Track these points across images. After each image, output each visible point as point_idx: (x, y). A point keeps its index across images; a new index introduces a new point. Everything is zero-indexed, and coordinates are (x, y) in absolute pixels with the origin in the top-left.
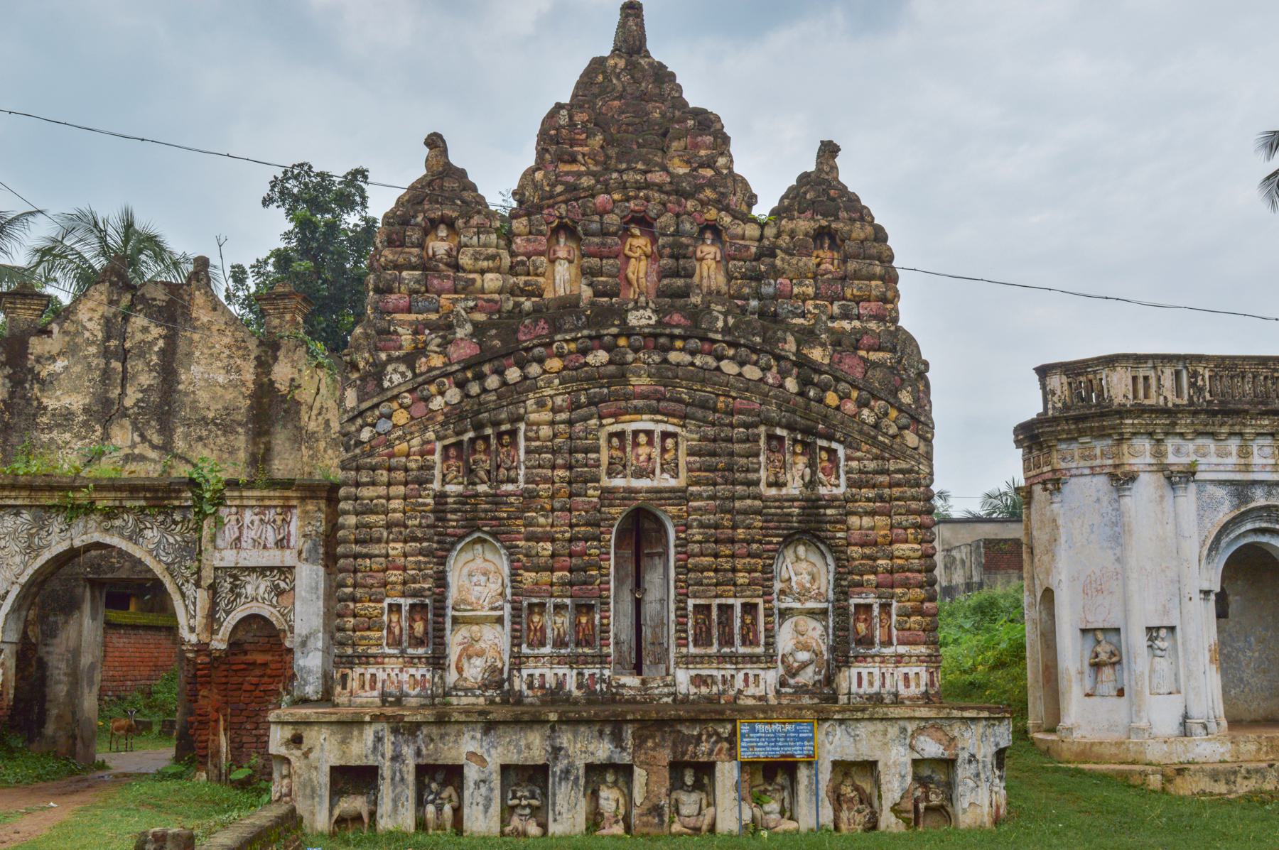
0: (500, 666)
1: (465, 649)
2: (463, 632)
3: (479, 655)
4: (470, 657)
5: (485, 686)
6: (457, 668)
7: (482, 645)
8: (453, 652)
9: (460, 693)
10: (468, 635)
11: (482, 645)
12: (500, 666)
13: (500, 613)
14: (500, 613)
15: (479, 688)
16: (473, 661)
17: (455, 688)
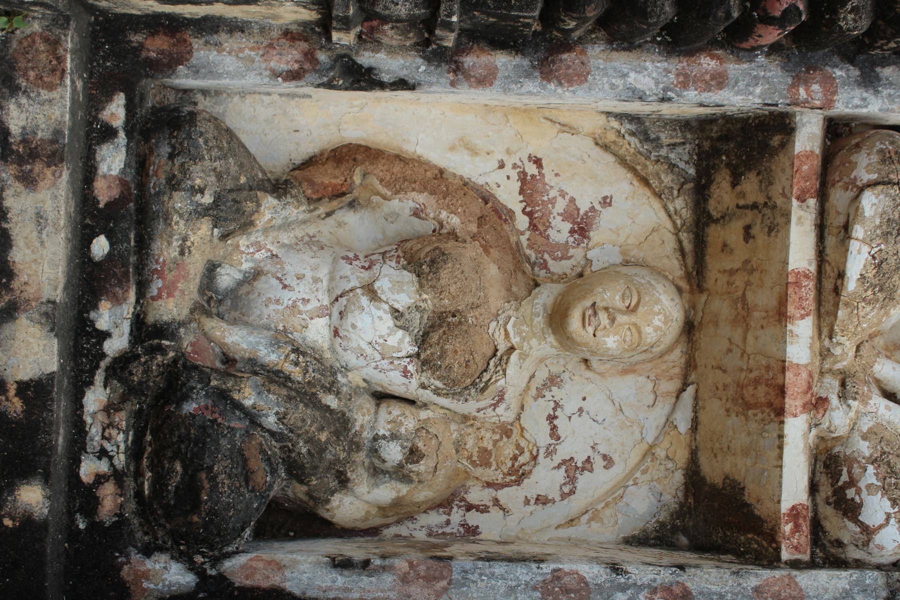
0: (345, 508)
1: (491, 212)
2: (635, 217)
3: (434, 336)
4: (422, 258)
5: (168, 391)
6: (347, 155)
7: (528, 348)
8: (465, 124)
9: (113, 160)
10: (603, 247)
11: (528, 348)
12: (345, 508)
13: (793, 543)
14: (793, 543)
15: (146, 332)
16: (399, 288)
17: (167, 127)
